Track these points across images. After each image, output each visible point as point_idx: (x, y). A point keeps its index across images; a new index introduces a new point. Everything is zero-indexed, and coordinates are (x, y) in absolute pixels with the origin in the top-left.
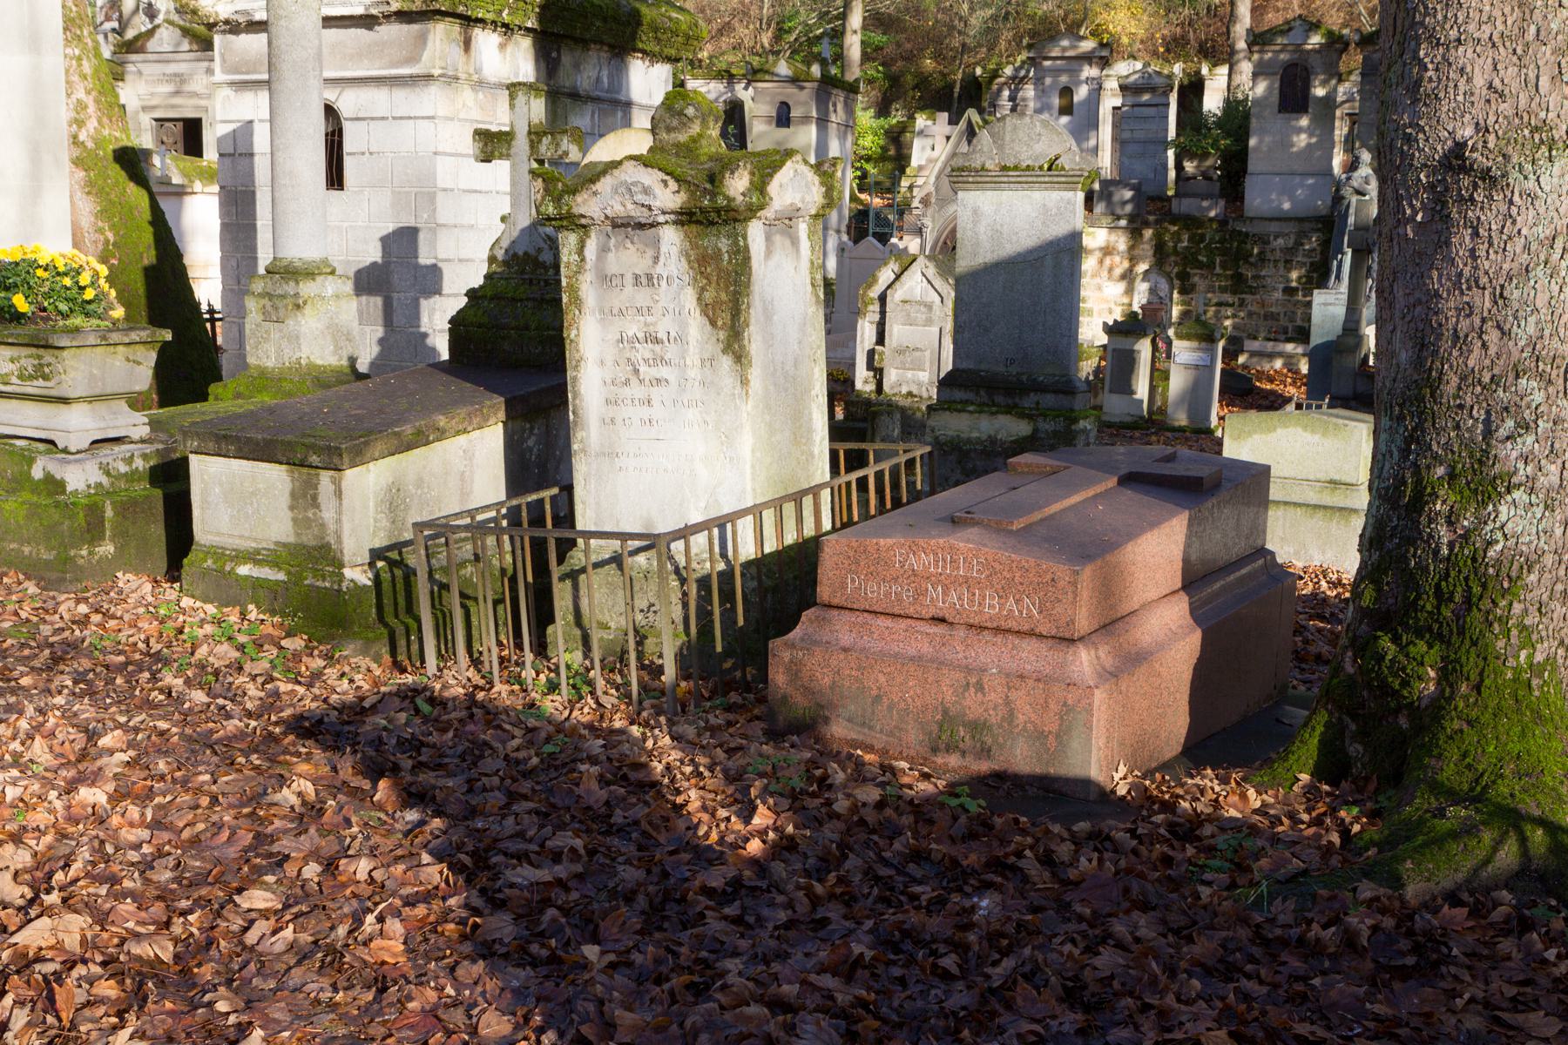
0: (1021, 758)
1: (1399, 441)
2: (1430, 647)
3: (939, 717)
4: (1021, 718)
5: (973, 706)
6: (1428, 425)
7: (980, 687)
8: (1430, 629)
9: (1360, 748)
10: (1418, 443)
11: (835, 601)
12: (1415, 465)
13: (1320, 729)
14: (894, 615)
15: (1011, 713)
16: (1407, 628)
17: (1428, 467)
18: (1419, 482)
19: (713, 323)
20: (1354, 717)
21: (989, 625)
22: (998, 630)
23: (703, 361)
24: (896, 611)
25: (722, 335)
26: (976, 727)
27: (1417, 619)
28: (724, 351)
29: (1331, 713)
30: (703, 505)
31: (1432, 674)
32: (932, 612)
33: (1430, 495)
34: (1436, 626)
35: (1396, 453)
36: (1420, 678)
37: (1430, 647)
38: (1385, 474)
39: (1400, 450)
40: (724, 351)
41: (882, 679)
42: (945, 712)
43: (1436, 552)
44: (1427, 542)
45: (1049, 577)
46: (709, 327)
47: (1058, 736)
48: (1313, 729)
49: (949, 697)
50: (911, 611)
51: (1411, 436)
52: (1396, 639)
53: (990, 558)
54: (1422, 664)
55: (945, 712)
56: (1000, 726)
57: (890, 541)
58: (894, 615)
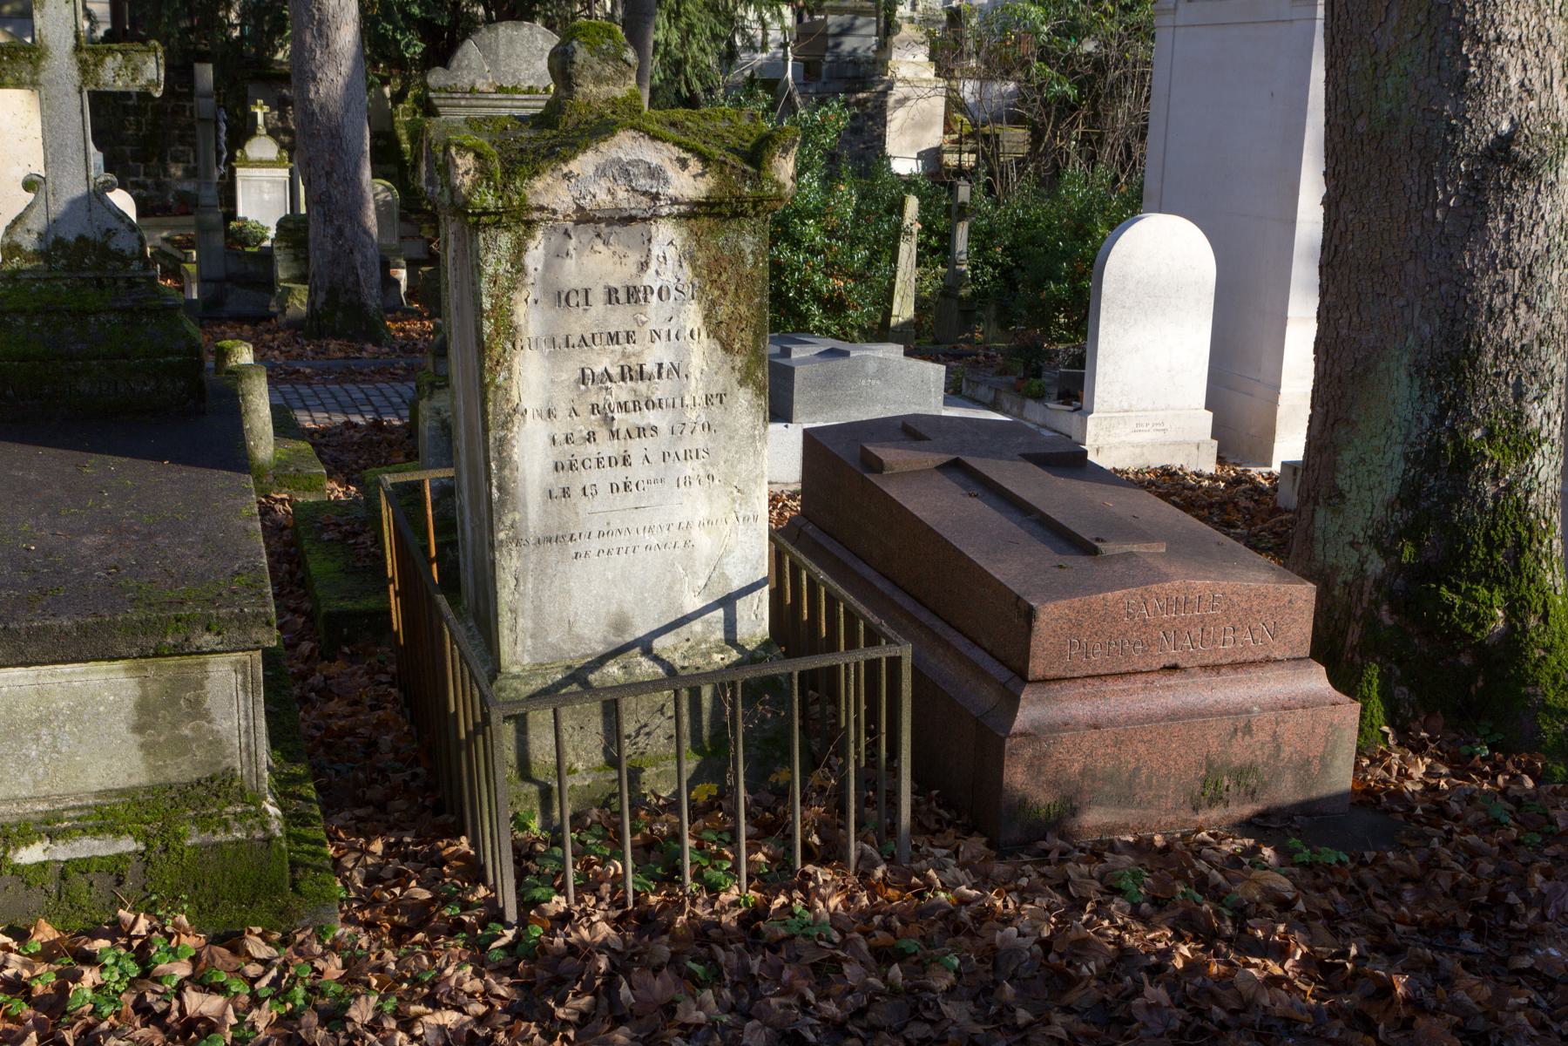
0: (1286, 792)
1: (1432, 408)
2: (1491, 590)
3: (1203, 772)
4: (1286, 752)
5: (1240, 752)
6: (1469, 392)
7: (1248, 730)
8: (1486, 574)
9: (1405, 690)
10: (1455, 410)
11: (1052, 673)
12: (1451, 429)
13: (1376, 682)
14: (1121, 675)
15: (1278, 748)
16: (1460, 577)
17: (1466, 431)
18: (1458, 444)
19: (727, 347)
20: (1400, 662)
21: (1224, 661)
22: (1236, 666)
23: (708, 399)
24: (1124, 669)
25: (739, 361)
26: (1240, 773)
27: (1469, 567)
28: (741, 383)
29: (1380, 665)
30: (702, 583)
31: (1500, 613)
32: (1165, 661)
33: (1476, 454)
34: (1491, 571)
35: (1427, 421)
36: (1493, 619)
37: (1491, 590)
38: (1412, 438)
39: (1433, 417)
40: (741, 383)
41: (1142, 749)
42: (1210, 765)
43: (1483, 503)
44: (1473, 499)
45: (1287, 598)
46: (720, 352)
47: (1322, 758)
48: (1370, 683)
49: (1214, 748)
50: (1140, 666)
51: (1449, 404)
52: (1454, 588)
53: (1228, 591)
54: (1492, 606)
55: (1210, 765)
56: (1266, 764)
57: (1118, 593)
58: (1121, 675)
